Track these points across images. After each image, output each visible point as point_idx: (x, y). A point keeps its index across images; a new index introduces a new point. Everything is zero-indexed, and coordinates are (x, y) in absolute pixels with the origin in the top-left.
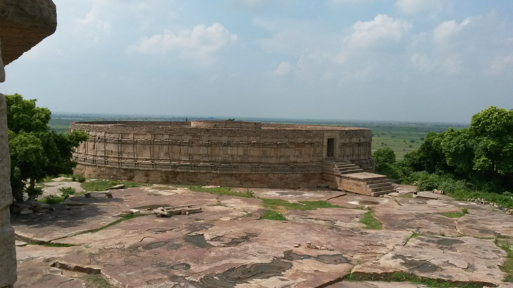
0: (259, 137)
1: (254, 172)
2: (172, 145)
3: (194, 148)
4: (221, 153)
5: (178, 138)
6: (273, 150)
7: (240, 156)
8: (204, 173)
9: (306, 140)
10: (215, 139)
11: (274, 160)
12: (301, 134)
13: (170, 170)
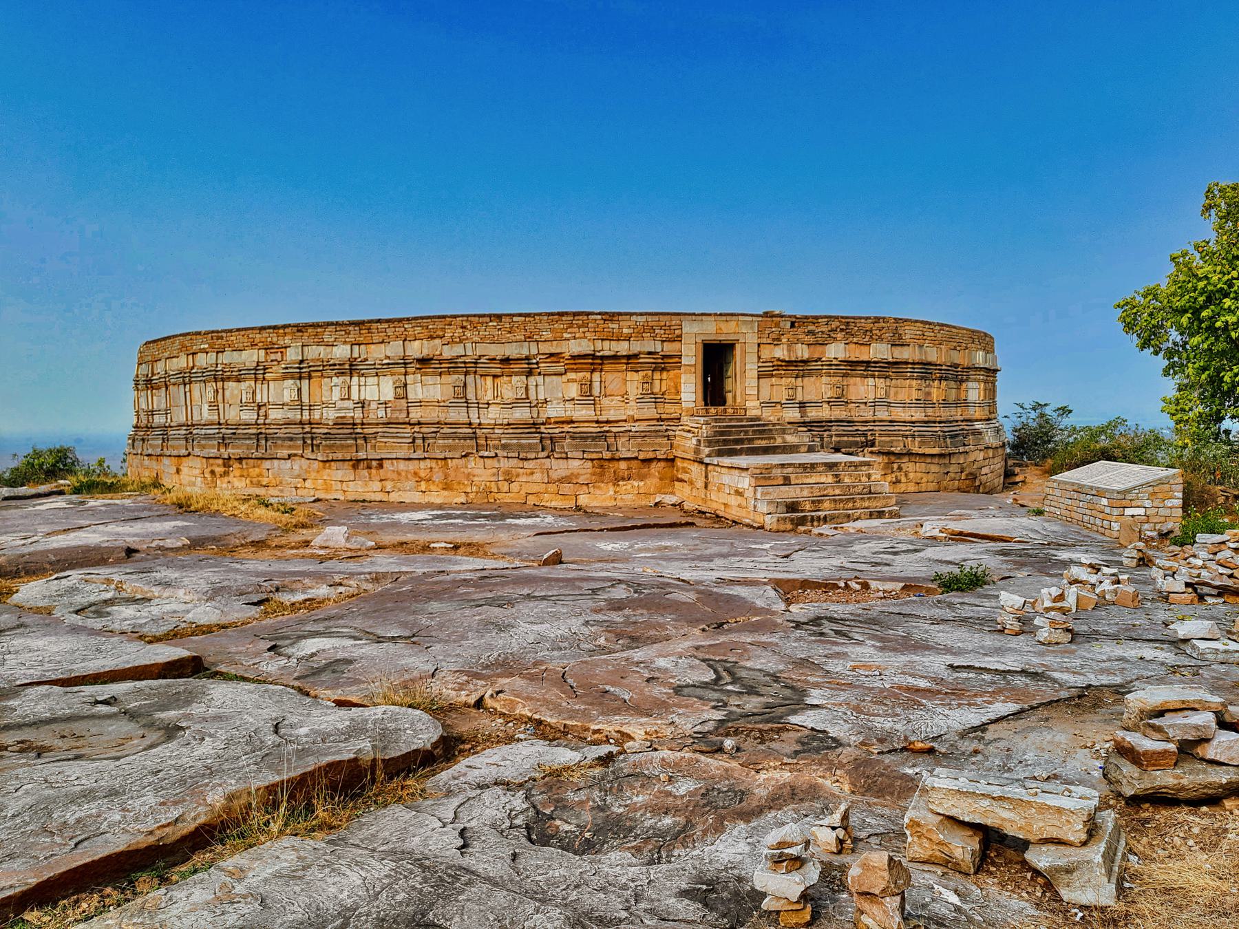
0: (437, 341)
1: (419, 454)
2: (223, 380)
6: (489, 379)
9: (599, 344)
11: (493, 415)
12: (585, 325)
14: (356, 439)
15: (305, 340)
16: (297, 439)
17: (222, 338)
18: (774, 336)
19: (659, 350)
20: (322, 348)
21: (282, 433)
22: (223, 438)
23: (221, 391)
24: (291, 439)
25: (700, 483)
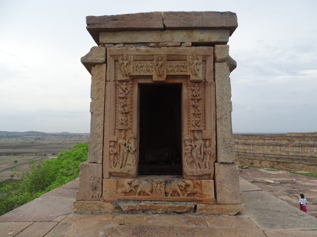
2: (275, 146)
3: (290, 148)
4: (309, 151)
5: (279, 142)
8: (297, 163)
10: (303, 142)
13: (274, 160)
15: (300, 139)
16: (301, 159)
17: (274, 137)
20: (304, 141)
21: (295, 158)
22: (277, 158)
24: (298, 159)
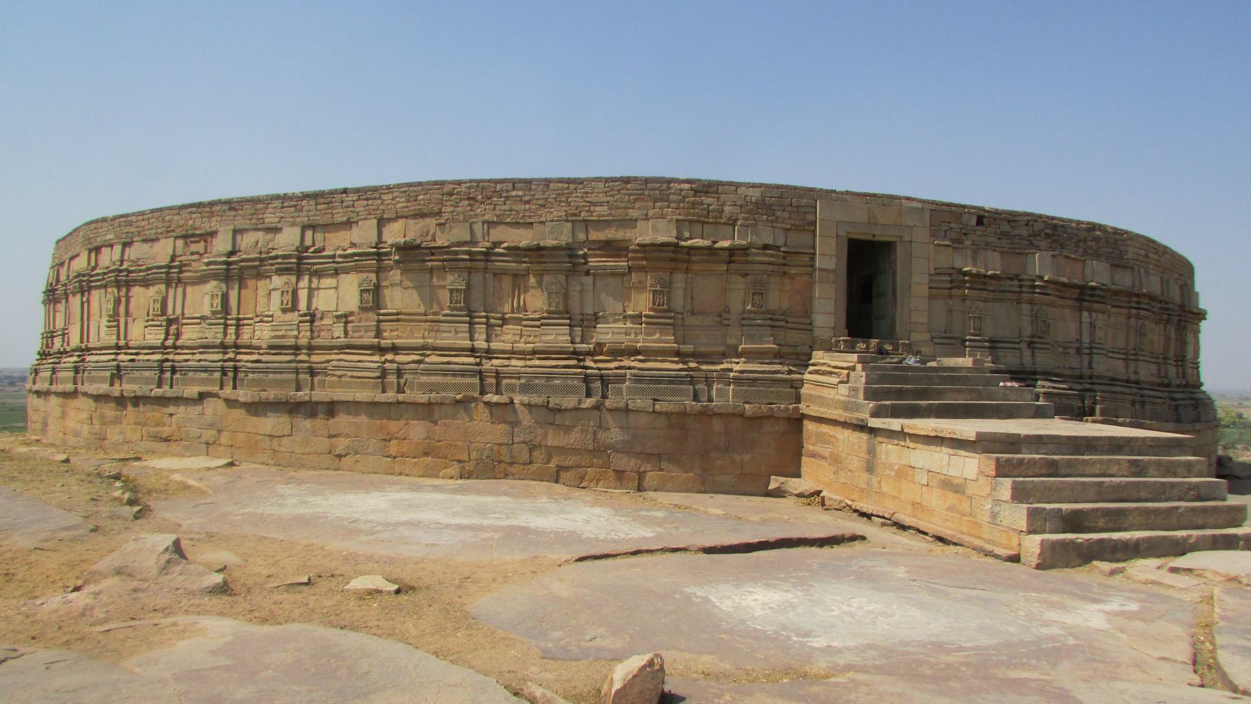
1: (391, 396)
7: (345, 318)
14: (297, 371)
18: (954, 236)
19: (780, 242)
20: (260, 234)
23: (123, 300)
25: (856, 462)
